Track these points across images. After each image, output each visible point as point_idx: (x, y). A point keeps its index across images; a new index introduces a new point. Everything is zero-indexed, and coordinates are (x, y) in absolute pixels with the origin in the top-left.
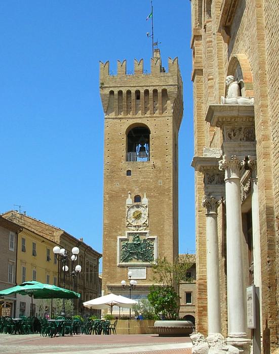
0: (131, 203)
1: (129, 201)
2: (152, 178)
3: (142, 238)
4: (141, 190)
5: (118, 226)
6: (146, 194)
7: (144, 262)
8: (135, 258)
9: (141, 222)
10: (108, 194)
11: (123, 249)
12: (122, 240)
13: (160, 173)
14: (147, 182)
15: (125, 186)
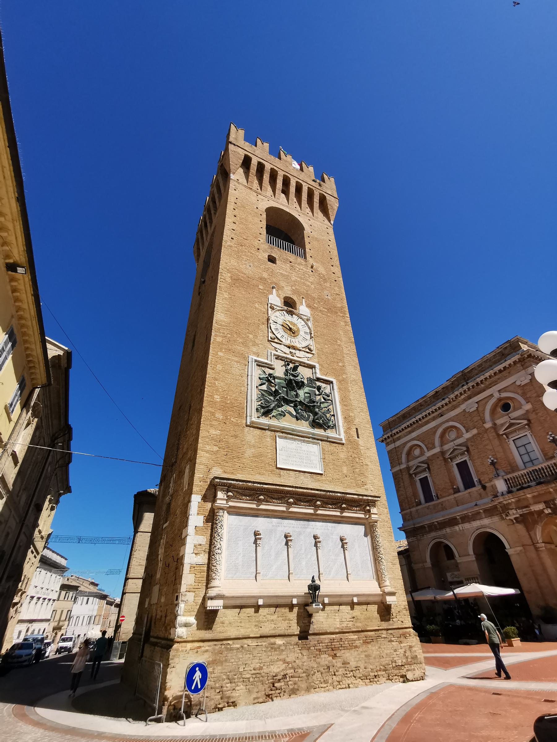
0: (279, 305)
1: (275, 299)
2: (312, 283)
3: (304, 373)
4: (295, 292)
6: (306, 302)
8: (290, 413)
9: (300, 342)
12: (260, 365)
13: (325, 281)
14: (304, 283)
15: (265, 275)
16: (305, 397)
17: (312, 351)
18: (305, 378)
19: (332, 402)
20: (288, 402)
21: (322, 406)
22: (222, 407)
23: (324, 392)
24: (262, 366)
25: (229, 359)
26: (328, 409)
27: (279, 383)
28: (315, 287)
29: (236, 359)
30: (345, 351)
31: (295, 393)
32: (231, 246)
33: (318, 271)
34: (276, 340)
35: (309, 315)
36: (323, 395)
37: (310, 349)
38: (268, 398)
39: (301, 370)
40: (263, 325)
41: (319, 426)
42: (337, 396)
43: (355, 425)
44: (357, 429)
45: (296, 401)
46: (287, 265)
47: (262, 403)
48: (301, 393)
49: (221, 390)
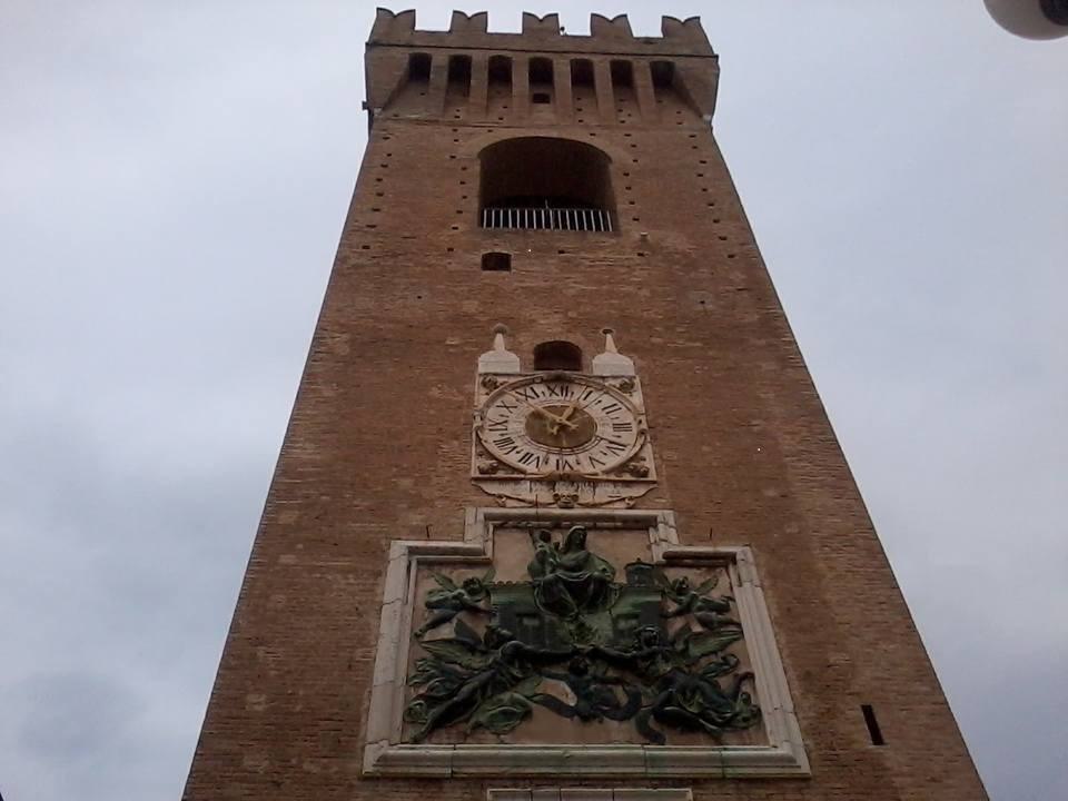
1: (500, 359)
2: (640, 285)
3: (614, 553)
5: (406, 483)
7: (656, 739)
9: (598, 459)
10: (344, 328)
11: (435, 624)
15: (471, 306)
16: (619, 633)
17: (645, 474)
18: (619, 566)
19: (739, 625)
20: (538, 663)
21: (695, 651)
22: (273, 728)
23: (705, 601)
24: (442, 564)
25: (312, 570)
26: (724, 658)
27: (506, 607)
28: (652, 292)
29: (343, 563)
30: (787, 443)
31: (572, 627)
32: (363, 266)
33: (662, 248)
34: (501, 474)
35: (633, 374)
36: (700, 609)
37: (635, 472)
38: (457, 667)
39: (597, 544)
40: (456, 443)
41: (687, 726)
42: (753, 607)
43: (858, 694)
44: (868, 712)
45: (577, 652)
46: (550, 261)
47: (431, 689)
48: (601, 625)
49: (273, 673)
